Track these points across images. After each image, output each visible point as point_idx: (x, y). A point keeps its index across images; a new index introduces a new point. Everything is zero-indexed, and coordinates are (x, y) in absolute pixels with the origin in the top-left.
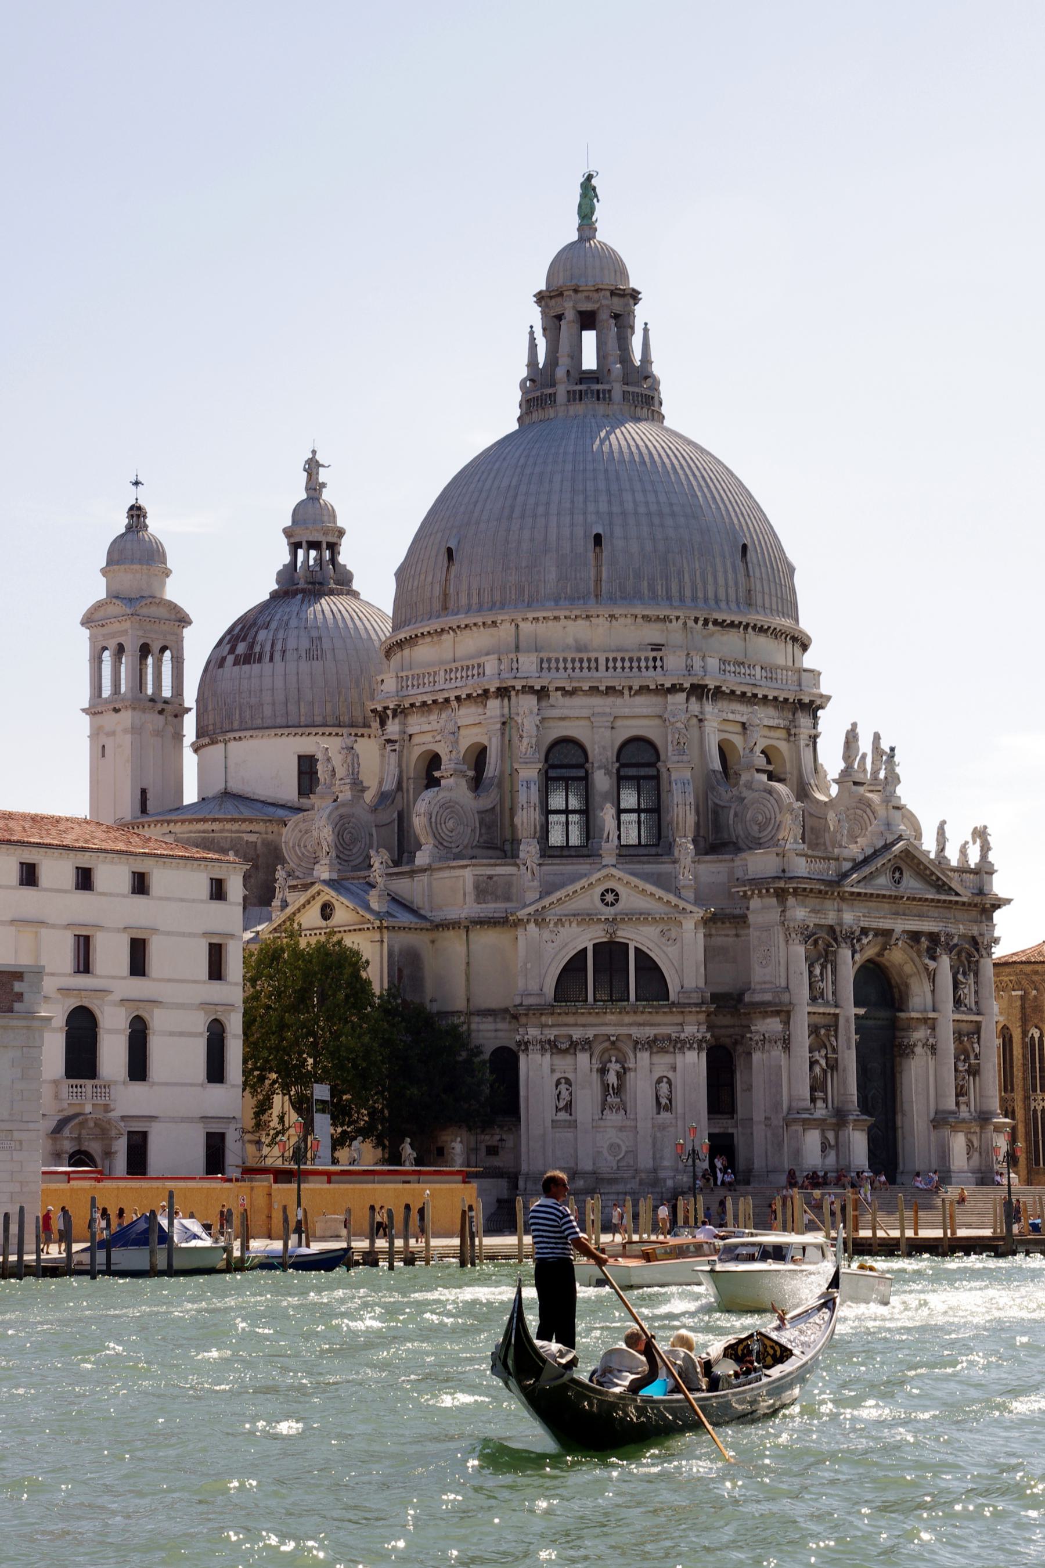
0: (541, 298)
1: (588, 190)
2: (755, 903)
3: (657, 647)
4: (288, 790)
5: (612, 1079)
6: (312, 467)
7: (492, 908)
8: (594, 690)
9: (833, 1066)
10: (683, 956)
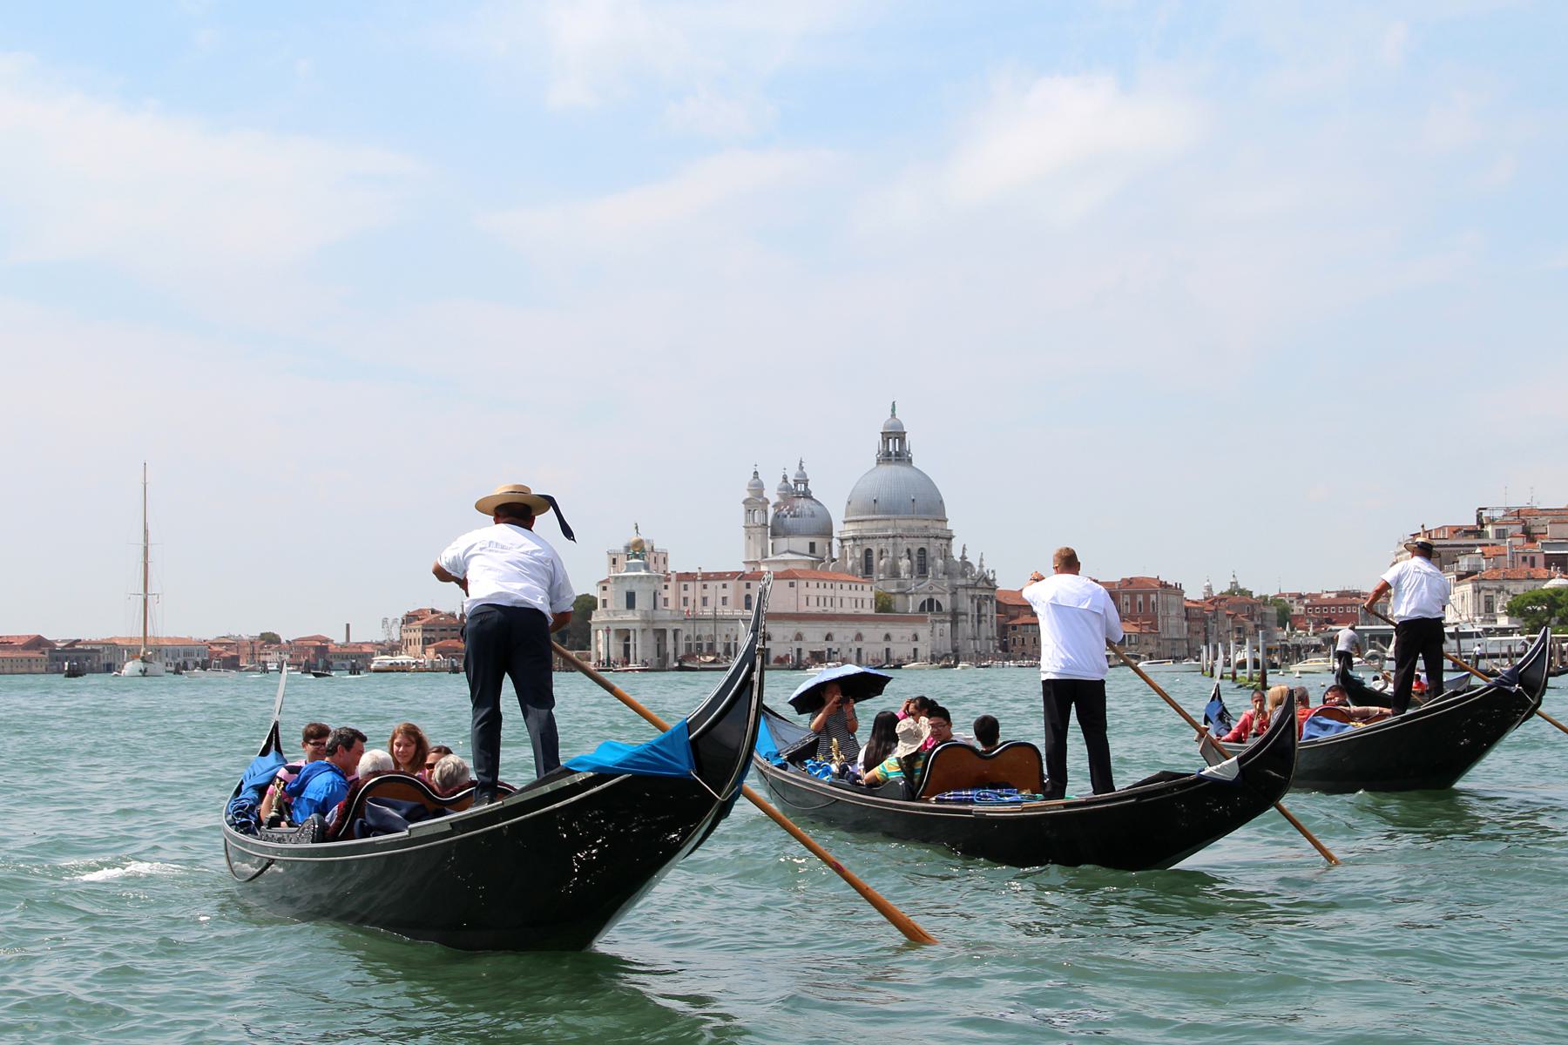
4: (807, 551)
10: (946, 603)
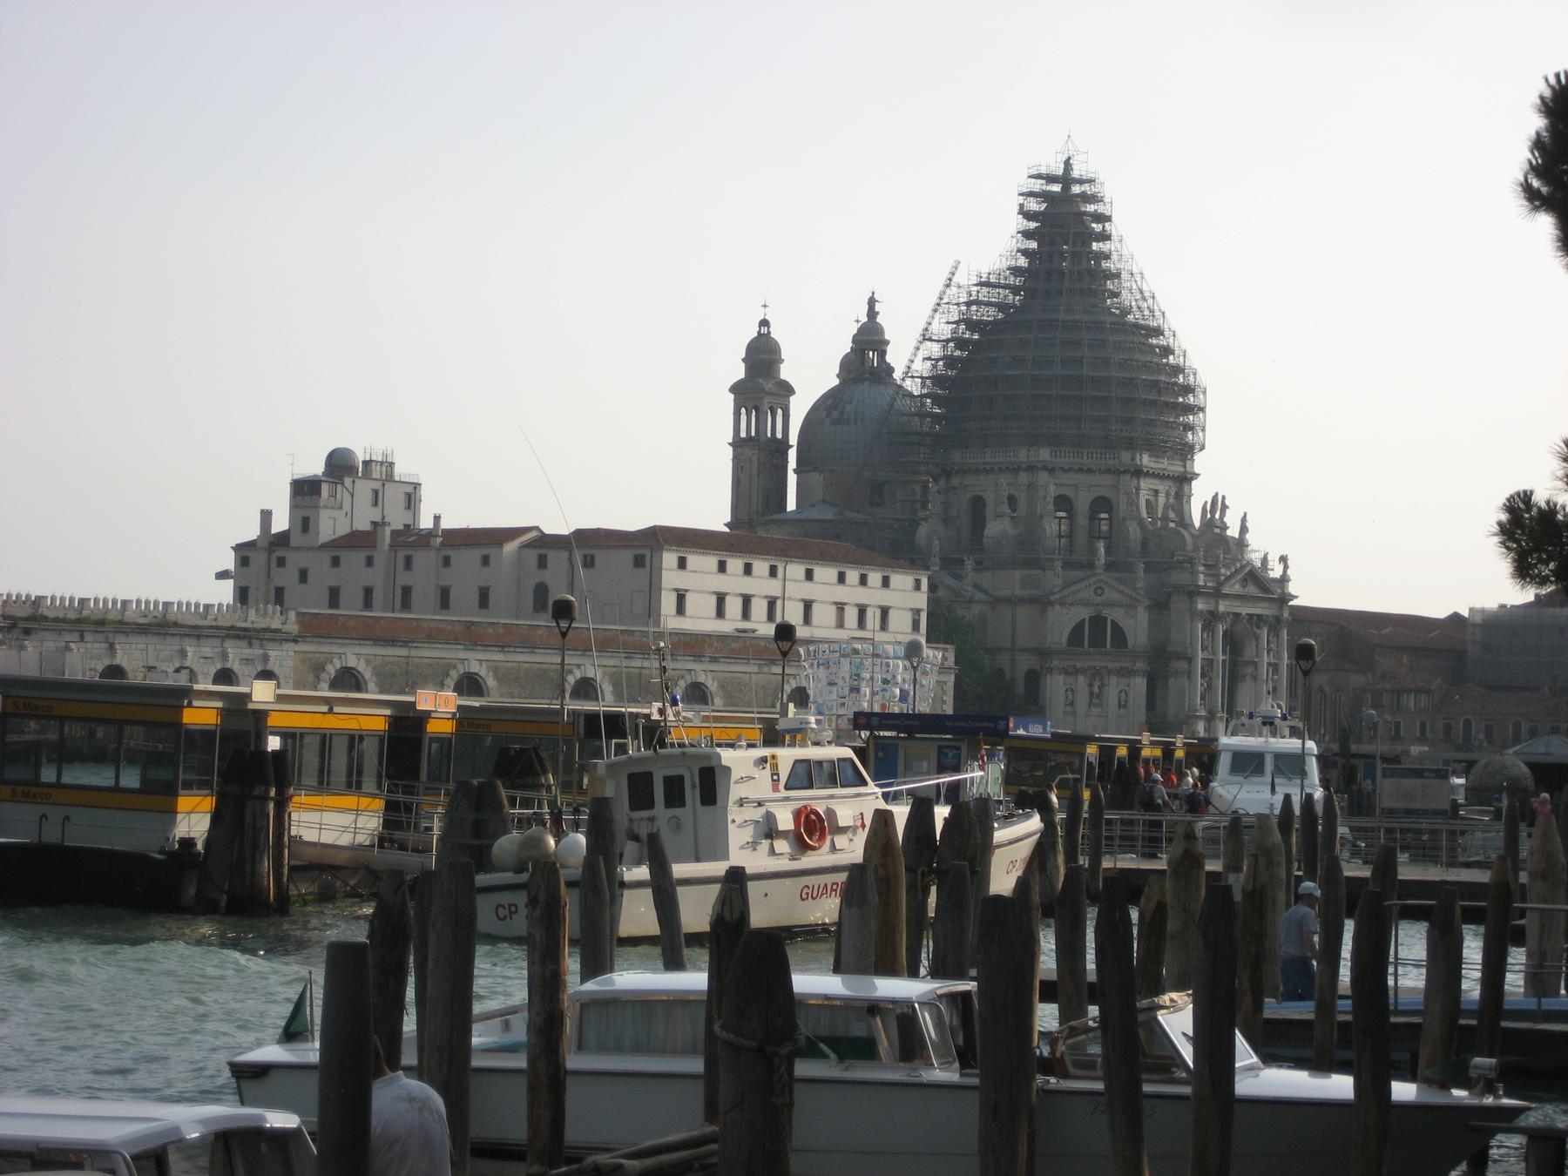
2: (1175, 598)
5: (1096, 689)
6: (872, 302)
8: (1080, 470)
9: (1210, 687)
10: (1138, 627)
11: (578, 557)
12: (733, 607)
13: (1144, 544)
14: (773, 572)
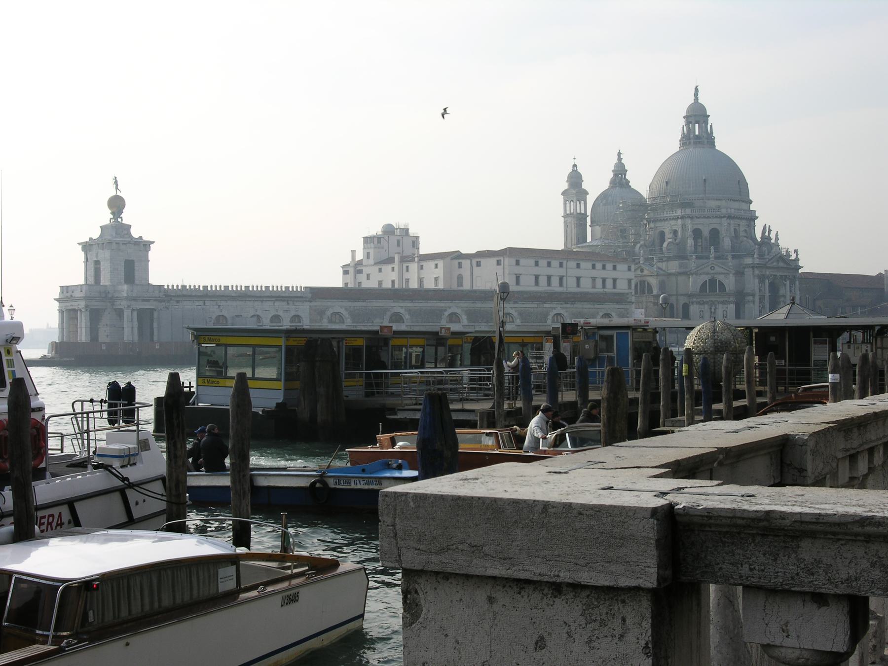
0: (684, 117)
1: (696, 89)
3: (719, 207)
6: (619, 154)
7: (682, 270)
8: (704, 217)
9: (764, 307)
10: (730, 283)
11: (474, 264)
12: (543, 281)
13: (733, 247)
14: (561, 265)
